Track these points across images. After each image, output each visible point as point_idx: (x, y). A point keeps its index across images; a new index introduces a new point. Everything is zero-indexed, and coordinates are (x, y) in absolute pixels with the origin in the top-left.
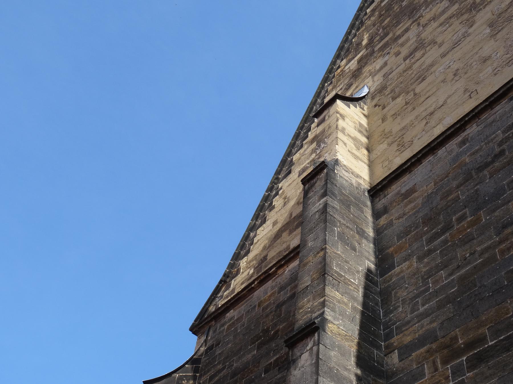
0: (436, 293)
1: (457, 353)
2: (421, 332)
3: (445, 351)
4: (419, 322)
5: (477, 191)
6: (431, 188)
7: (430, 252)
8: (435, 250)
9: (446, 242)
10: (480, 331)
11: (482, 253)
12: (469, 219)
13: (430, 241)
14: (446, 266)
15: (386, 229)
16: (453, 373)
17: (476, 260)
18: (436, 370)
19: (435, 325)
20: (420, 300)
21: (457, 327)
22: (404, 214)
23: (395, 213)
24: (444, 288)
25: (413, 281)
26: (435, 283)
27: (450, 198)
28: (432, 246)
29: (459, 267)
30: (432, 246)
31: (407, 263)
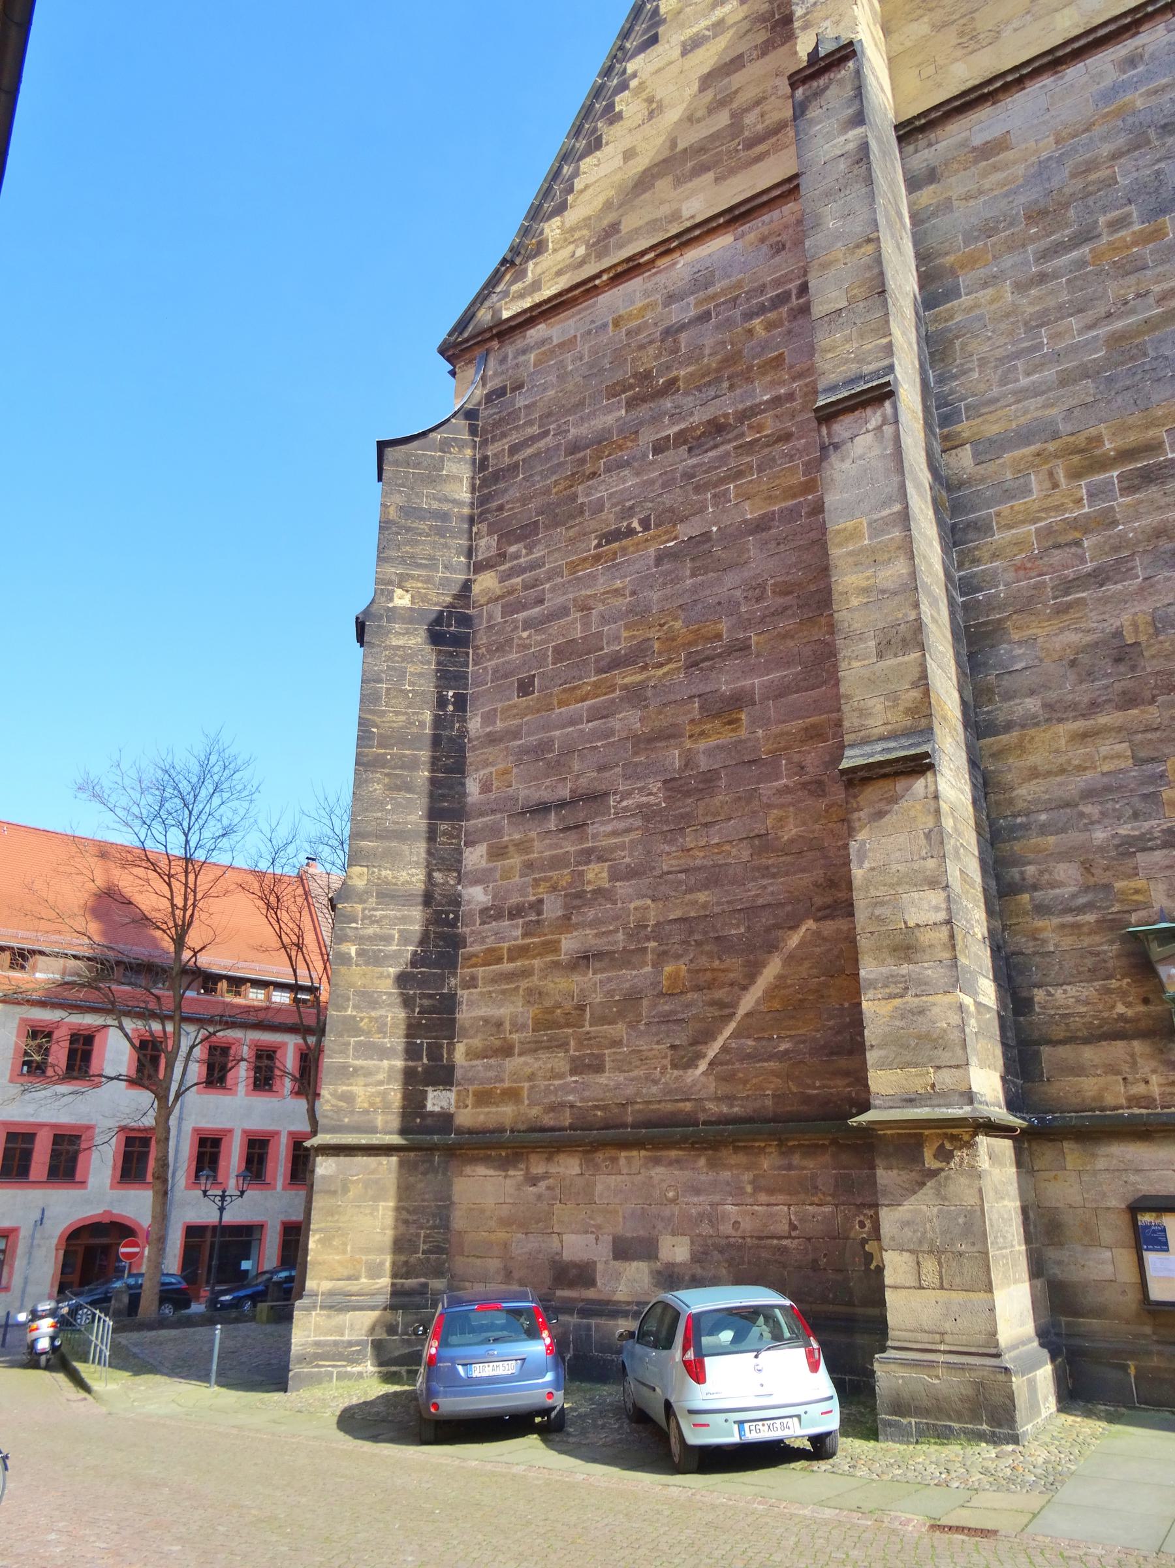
0: (1057, 356)
1: (1103, 464)
2: (1023, 420)
3: (1076, 458)
4: (1018, 401)
5: (1158, 173)
6: (1047, 147)
7: (1042, 278)
8: (1055, 276)
9: (1081, 263)
10: (1151, 433)
11: (1163, 298)
12: (1137, 227)
13: (1044, 255)
14: (1080, 311)
15: (934, 214)
16: (1091, 495)
17: (1149, 308)
18: (1055, 486)
19: (1053, 411)
20: (1020, 364)
21: (1101, 421)
22: (981, 192)
23: (956, 185)
24: (1073, 349)
25: (1003, 326)
26: (1056, 336)
27: (1093, 177)
28: (1049, 267)
29: (1109, 315)
30: (1049, 267)
31: (990, 292)
